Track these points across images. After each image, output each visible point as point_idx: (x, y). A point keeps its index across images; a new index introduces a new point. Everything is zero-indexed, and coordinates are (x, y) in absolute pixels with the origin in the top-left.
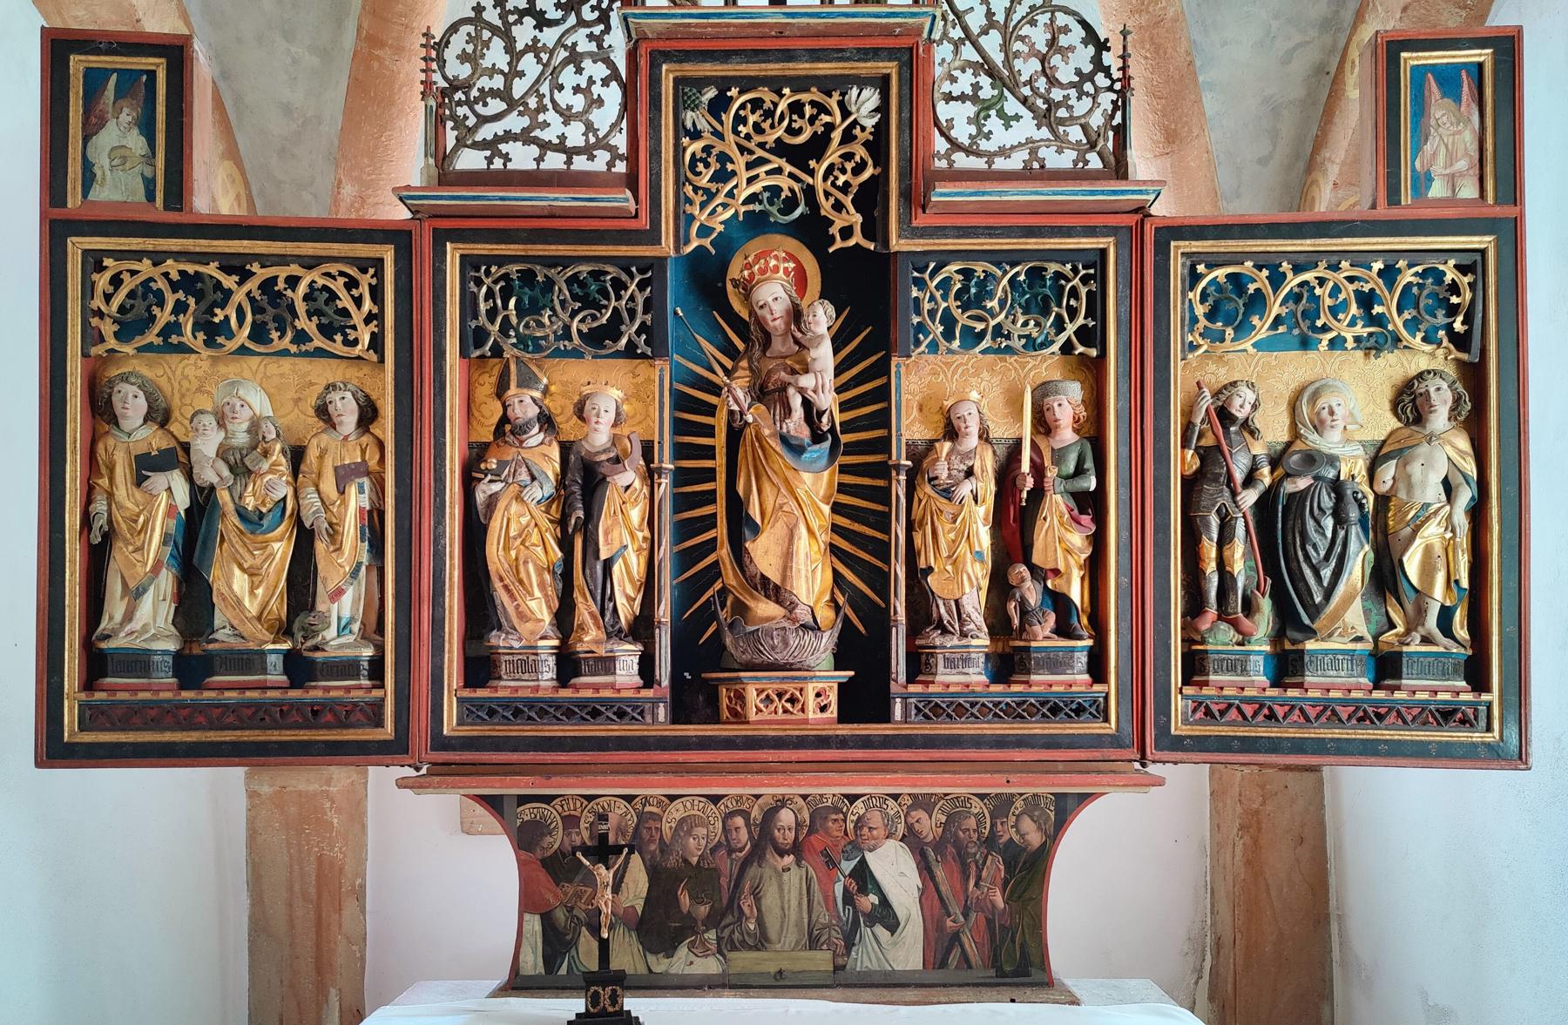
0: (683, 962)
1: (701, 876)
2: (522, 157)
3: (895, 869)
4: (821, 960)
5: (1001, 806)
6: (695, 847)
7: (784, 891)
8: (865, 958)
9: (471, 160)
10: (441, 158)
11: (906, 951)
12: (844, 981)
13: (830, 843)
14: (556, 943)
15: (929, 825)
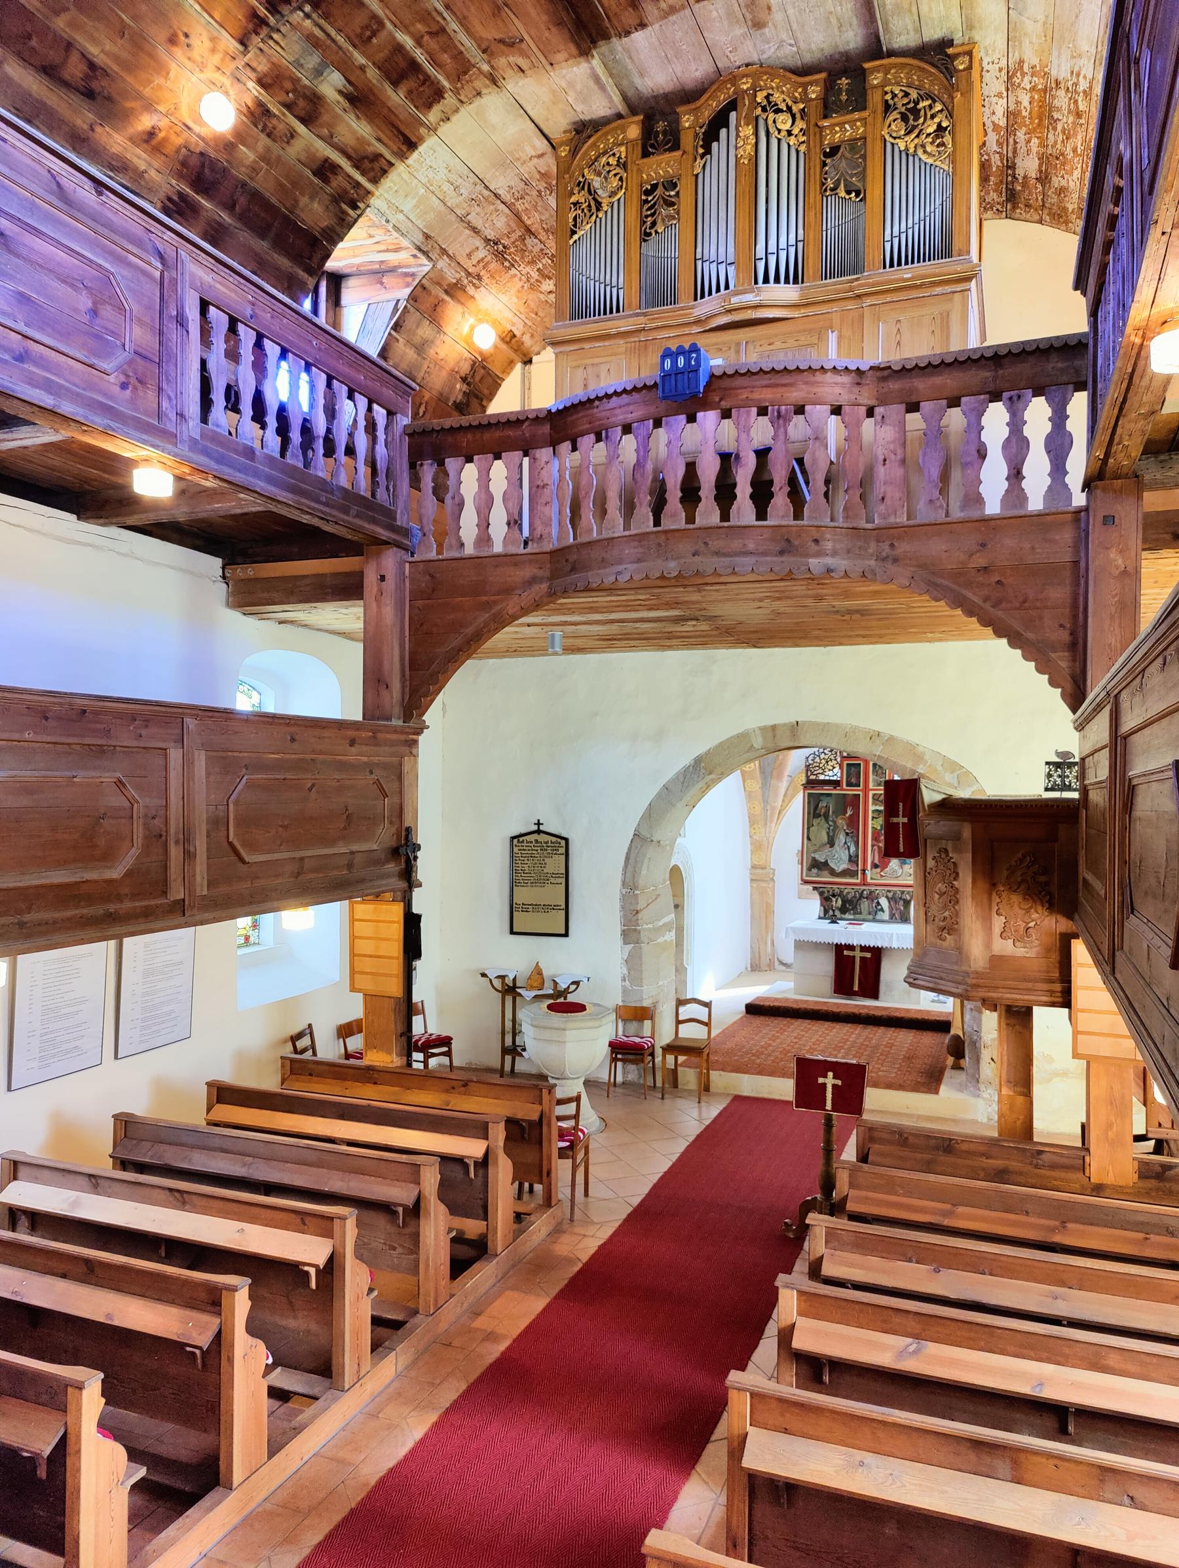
0: (847, 916)
1: (850, 902)
2: (822, 777)
3: (884, 902)
4: (871, 917)
5: (903, 892)
6: (849, 897)
7: (865, 905)
8: (878, 917)
9: (813, 777)
10: (807, 777)
11: (886, 916)
12: (874, 920)
13: (872, 897)
14: (826, 912)
15: (890, 895)
